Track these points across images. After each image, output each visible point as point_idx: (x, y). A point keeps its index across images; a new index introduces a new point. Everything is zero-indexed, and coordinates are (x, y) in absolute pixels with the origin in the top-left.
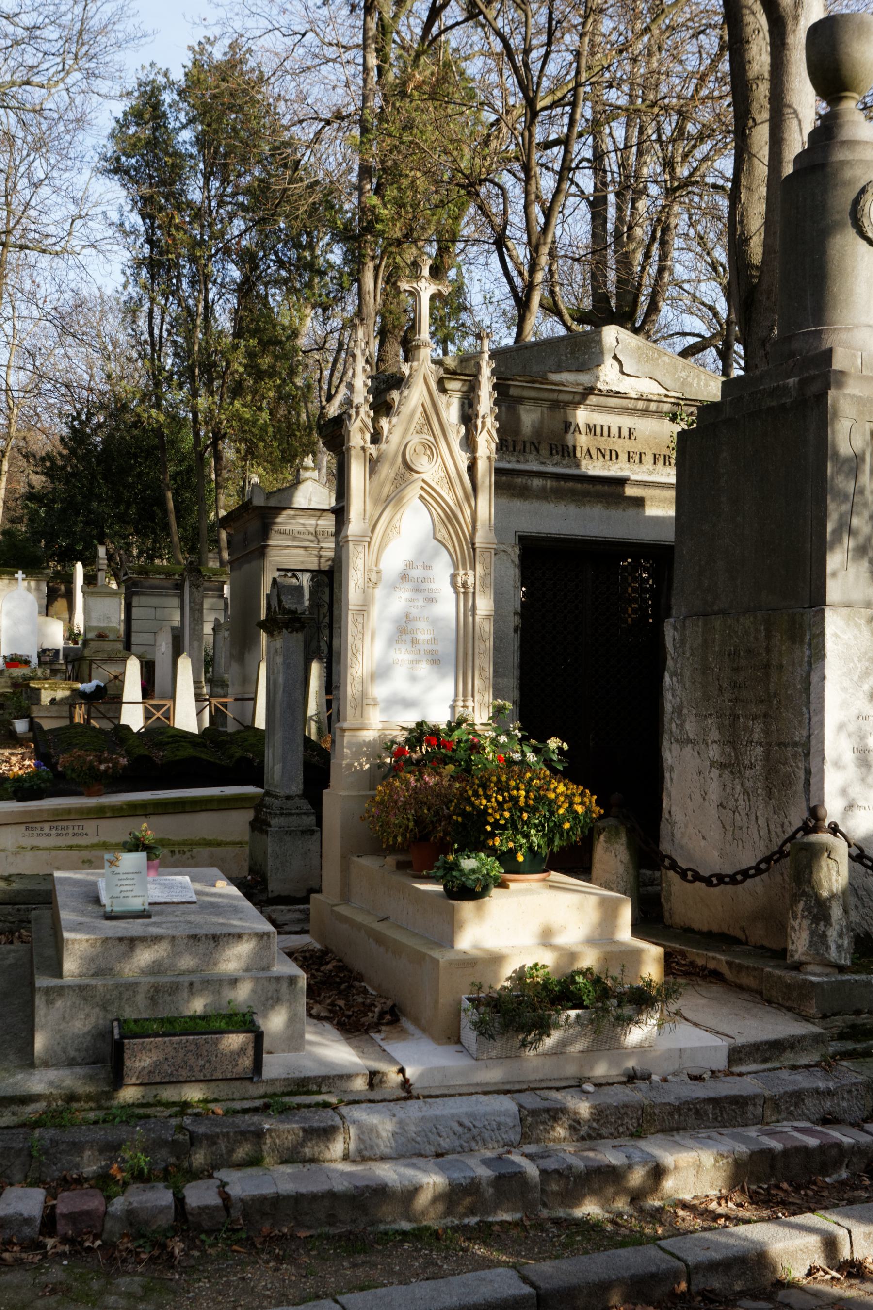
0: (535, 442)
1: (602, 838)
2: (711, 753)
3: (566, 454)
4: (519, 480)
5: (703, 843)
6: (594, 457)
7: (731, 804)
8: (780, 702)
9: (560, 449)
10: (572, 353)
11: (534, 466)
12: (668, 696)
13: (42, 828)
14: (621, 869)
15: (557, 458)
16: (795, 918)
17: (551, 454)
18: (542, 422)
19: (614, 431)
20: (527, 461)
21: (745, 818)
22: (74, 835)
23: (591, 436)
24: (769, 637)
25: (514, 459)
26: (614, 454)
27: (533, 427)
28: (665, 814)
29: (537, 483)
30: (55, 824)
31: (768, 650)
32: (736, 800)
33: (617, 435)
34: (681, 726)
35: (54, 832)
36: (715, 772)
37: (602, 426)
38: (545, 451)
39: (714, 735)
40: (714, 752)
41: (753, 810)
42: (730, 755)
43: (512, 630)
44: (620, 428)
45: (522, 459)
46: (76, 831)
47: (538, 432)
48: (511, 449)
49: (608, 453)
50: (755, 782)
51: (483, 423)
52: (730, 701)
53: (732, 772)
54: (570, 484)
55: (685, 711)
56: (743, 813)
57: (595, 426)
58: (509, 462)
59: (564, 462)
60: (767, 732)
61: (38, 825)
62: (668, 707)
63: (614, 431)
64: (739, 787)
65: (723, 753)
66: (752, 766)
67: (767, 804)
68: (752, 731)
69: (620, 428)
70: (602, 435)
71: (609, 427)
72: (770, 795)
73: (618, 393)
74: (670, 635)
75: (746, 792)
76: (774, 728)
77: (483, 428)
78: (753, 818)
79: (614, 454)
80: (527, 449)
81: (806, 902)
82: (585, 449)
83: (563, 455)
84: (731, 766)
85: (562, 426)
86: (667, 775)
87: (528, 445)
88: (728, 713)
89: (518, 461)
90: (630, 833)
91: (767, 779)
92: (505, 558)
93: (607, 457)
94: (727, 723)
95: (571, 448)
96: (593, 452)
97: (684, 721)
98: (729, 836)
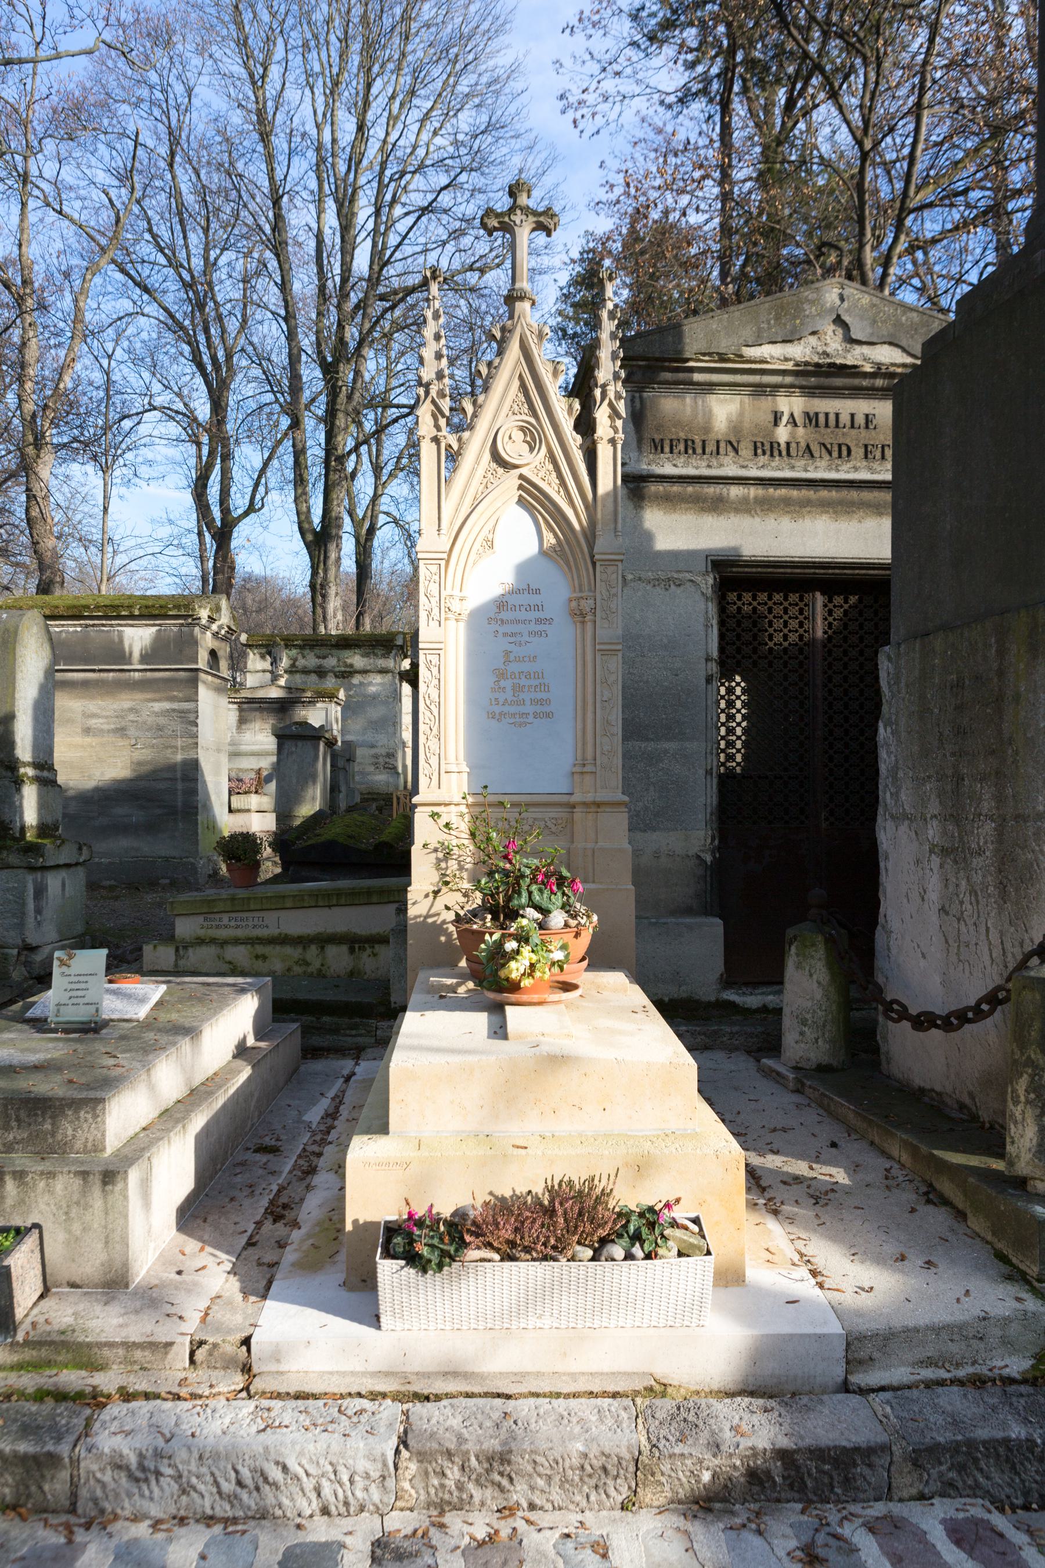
0: (733, 440)
1: (793, 949)
2: (931, 832)
3: (776, 453)
4: (711, 490)
5: (922, 963)
6: (816, 454)
7: (954, 909)
8: (1017, 752)
9: (767, 447)
10: (777, 318)
11: (731, 469)
12: (883, 754)
13: (220, 919)
14: (819, 994)
15: (762, 459)
16: (1016, 1102)
17: (756, 454)
18: (741, 414)
19: (845, 419)
20: (722, 465)
21: (972, 928)
22: (255, 926)
23: (811, 429)
24: (1002, 653)
25: (704, 464)
26: (844, 448)
27: (730, 421)
28: (881, 919)
29: (735, 492)
30: (233, 915)
31: (1001, 673)
32: (962, 903)
33: (848, 424)
34: (896, 795)
35: (233, 923)
36: (936, 860)
37: (827, 415)
38: (746, 451)
39: (934, 807)
40: (933, 831)
41: (982, 919)
42: (953, 836)
43: (703, 681)
44: (852, 415)
45: (714, 462)
46: (256, 922)
47: (736, 428)
48: (699, 451)
49: (836, 448)
50: (984, 876)
51: (604, 395)
52: (953, 754)
53: (956, 862)
54: (783, 492)
55: (901, 774)
56: (970, 922)
57: (817, 414)
58: (697, 468)
59: (773, 464)
60: (1000, 799)
61: (217, 916)
62: (883, 768)
63: (845, 419)
64: (964, 883)
65: (944, 833)
66: (980, 852)
67: (1001, 910)
68: (980, 799)
69: (852, 415)
70: (827, 425)
71: (837, 415)
72: (1004, 895)
73: (844, 367)
74: (885, 667)
75: (973, 892)
76: (1009, 791)
77: (602, 401)
78: (983, 930)
79: (844, 448)
80: (722, 450)
81: (1032, 1077)
82: (803, 445)
83: (772, 455)
84: (954, 852)
85: (771, 418)
86: (882, 865)
87: (722, 445)
88: (950, 772)
89: (709, 466)
90: (830, 941)
91: (1000, 871)
92: (693, 589)
93: (835, 454)
94: (949, 787)
95: (783, 446)
96: (815, 448)
97: (899, 789)
98: (953, 958)
